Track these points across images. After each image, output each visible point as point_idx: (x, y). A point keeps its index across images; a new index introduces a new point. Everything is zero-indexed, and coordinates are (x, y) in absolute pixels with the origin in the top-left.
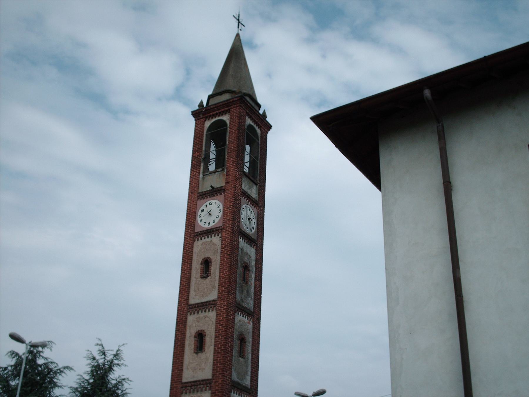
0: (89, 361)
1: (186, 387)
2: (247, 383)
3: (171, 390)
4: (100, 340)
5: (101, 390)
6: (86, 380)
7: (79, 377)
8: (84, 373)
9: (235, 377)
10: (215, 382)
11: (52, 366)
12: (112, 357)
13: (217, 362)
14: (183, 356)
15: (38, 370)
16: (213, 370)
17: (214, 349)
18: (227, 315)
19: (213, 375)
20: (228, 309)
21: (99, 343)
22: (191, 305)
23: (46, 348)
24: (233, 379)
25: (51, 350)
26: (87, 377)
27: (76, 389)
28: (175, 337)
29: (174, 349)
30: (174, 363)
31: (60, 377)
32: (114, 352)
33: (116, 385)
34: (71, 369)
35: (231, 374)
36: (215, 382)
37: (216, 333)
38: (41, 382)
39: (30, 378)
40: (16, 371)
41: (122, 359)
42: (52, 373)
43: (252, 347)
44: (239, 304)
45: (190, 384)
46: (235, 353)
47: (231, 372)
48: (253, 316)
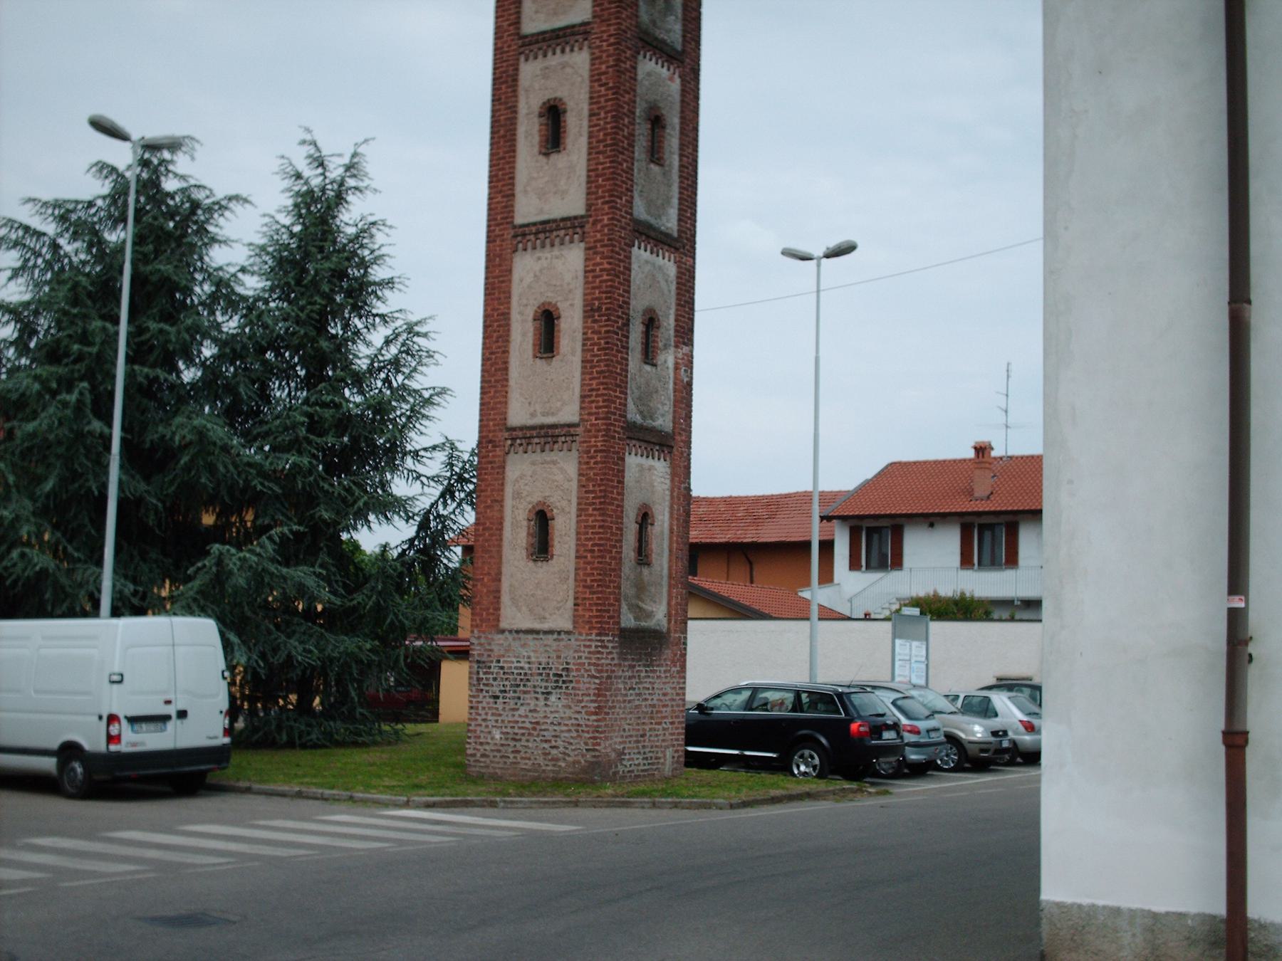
0: (288, 183)
1: (524, 235)
2: (669, 225)
3: (488, 242)
4: (308, 130)
5: (321, 250)
6: (284, 226)
7: (267, 220)
8: (279, 211)
9: (640, 210)
10: (595, 223)
11: (199, 195)
12: (341, 171)
13: (597, 176)
14: (514, 162)
15: (168, 206)
16: (588, 194)
17: (590, 143)
18: (618, 60)
19: (589, 207)
20: (618, 43)
21: (308, 137)
22: (526, 37)
23: (180, 154)
24: (636, 213)
25: (193, 158)
26: (287, 221)
27: (263, 248)
28: (493, 116)
29: (492, 144)
30: (494, 179)
31: (221, 221)
32: (346, 160)
33: (357, 236)
34: (246, 201)
35: (630, 202)
36: (595, 223)
37: (591, 104)
38: (179, 232)
39: (151, 224)
40: (117, 208)
41: (366, 175)
42: (200, 212)
43: (680, 139)
44: (646, 33)
45: (534, 229)
46: (640, 152)
47: (632, 197)
48: (682, 62)
